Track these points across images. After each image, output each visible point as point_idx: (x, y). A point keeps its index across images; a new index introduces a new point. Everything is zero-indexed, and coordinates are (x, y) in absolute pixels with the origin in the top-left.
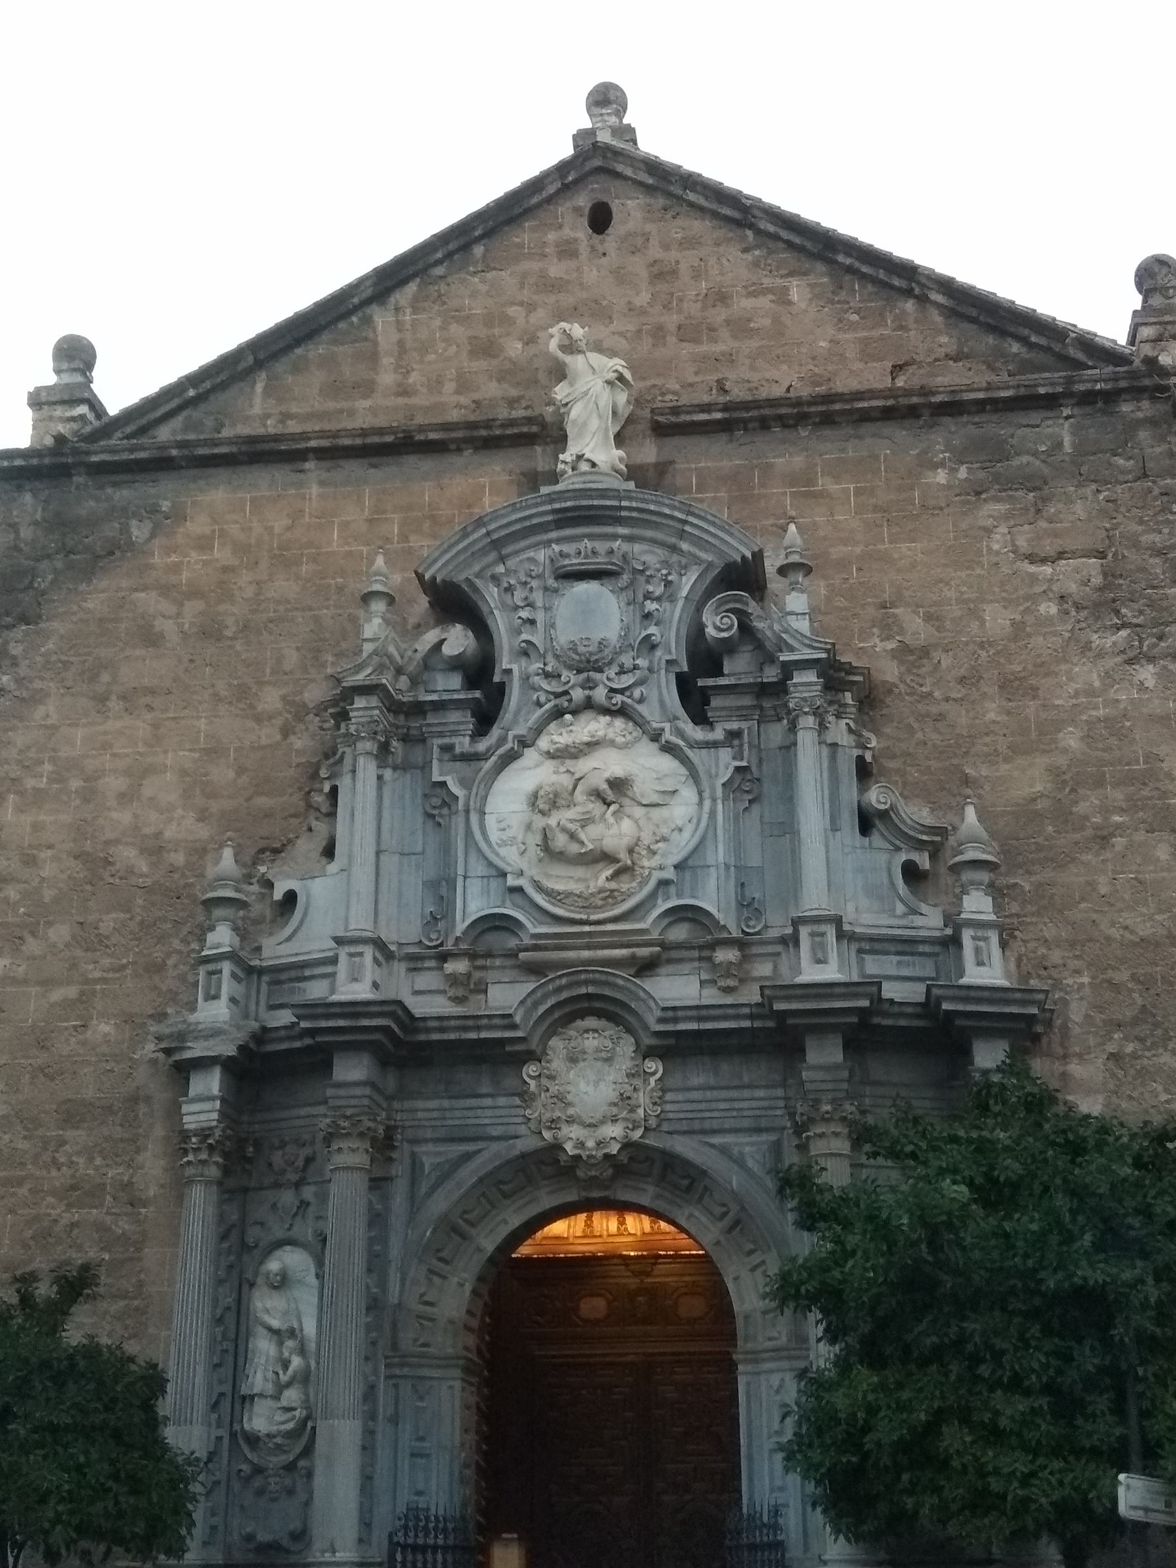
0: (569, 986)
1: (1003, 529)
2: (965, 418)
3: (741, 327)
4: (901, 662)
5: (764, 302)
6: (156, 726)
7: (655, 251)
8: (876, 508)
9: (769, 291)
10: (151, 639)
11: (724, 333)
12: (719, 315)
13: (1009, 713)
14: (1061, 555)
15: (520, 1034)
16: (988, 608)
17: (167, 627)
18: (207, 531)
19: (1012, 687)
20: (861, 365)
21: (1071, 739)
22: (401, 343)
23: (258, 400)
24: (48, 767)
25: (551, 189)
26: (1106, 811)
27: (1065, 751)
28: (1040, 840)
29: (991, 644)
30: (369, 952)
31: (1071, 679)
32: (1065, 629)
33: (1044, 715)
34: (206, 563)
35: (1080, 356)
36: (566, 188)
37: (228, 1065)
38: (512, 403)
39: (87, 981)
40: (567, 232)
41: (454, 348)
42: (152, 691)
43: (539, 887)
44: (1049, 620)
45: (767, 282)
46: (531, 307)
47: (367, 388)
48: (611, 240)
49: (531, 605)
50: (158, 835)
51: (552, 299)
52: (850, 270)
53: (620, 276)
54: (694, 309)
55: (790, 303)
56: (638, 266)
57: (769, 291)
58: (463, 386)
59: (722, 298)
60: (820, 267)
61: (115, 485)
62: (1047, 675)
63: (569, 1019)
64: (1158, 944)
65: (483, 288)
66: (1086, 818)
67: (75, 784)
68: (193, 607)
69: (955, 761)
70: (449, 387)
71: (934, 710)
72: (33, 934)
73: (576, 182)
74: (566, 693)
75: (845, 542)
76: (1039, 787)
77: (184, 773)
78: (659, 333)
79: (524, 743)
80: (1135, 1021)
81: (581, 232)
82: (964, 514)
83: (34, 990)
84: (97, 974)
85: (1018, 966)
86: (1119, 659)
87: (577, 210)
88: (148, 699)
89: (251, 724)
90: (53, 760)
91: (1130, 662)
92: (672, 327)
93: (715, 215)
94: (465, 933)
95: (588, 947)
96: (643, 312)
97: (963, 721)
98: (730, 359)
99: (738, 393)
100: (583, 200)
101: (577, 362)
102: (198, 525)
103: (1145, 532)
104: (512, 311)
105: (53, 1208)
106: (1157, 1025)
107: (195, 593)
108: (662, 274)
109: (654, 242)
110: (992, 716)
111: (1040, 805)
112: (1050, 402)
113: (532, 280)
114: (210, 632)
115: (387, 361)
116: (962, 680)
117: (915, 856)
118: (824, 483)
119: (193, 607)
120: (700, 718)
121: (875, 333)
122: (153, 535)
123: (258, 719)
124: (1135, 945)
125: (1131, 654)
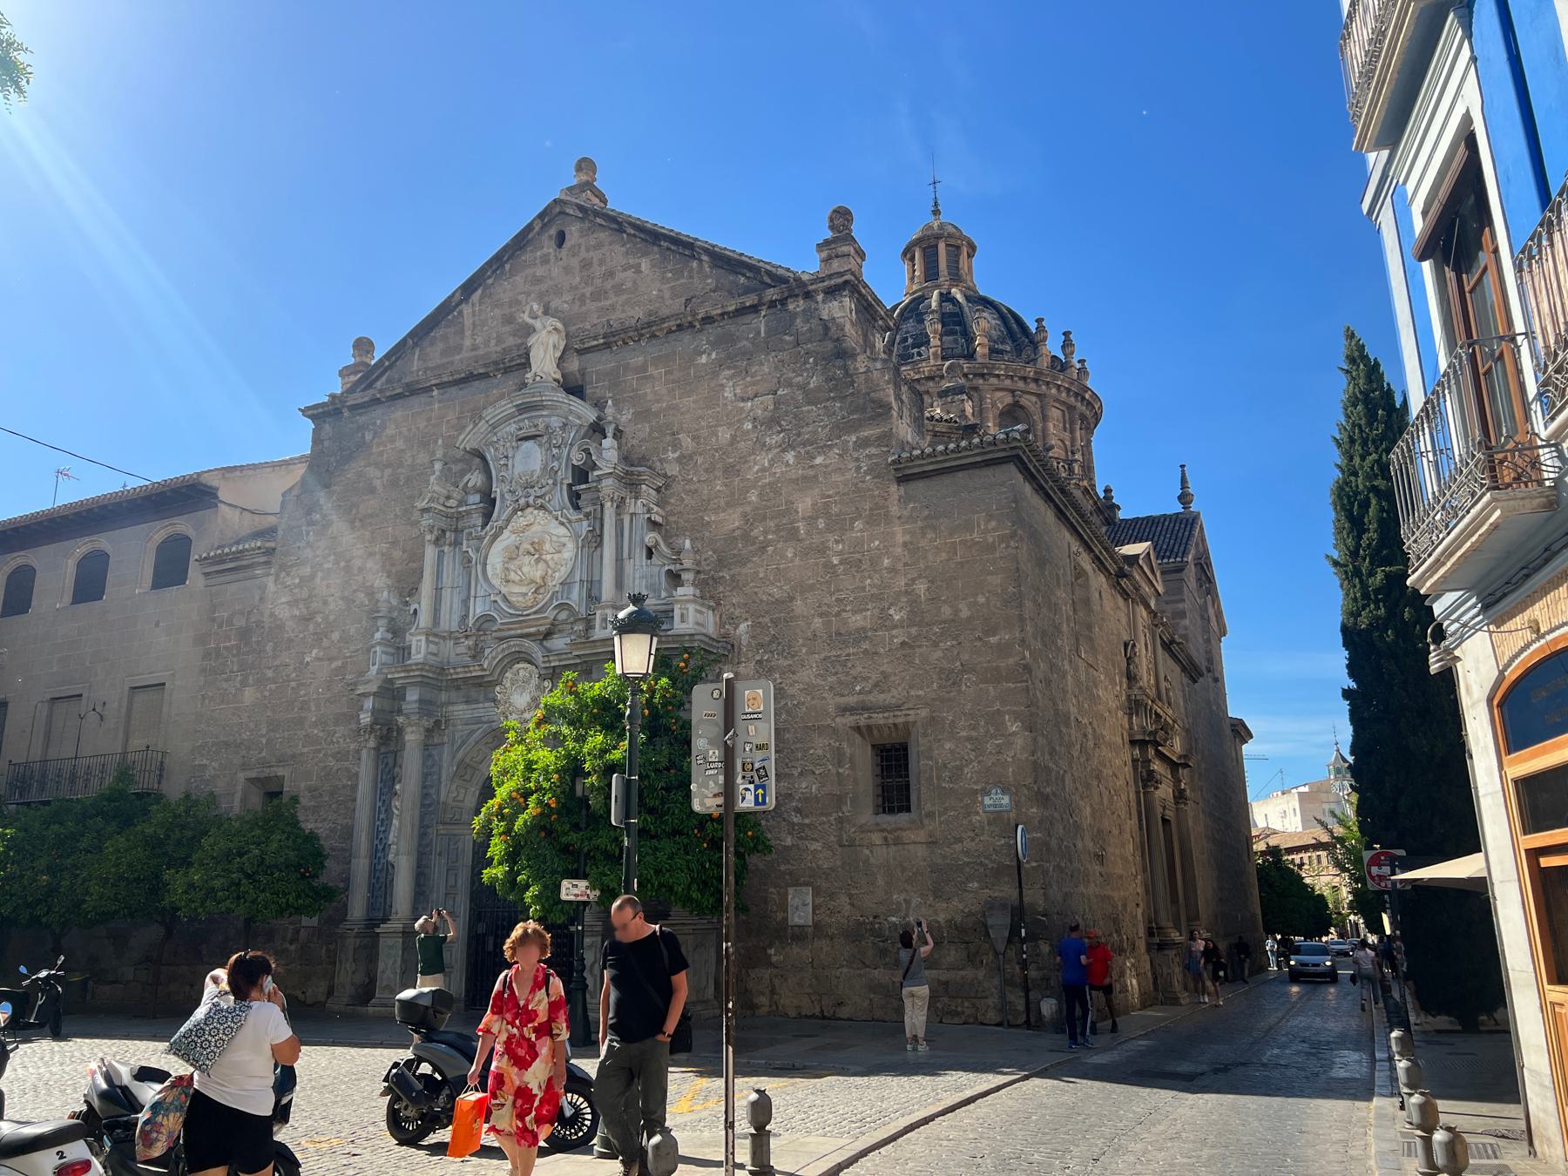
0: (508, 648)
1: (731, 384)
2: (716, 324)
3: (618, 289)
4: (681, 464)
5: (630, 273)
6: (373, 533)
7: (583, 254)
8: (673, 381)
9: (632, 267)
10: (372, 490)
11: (611, 294)
12: (609, 285)
13: (726, 486)
14: (756, 396)
15: (488, 673)
16: (720, 429)
17: (377, 483)
18: (394, 432)
19: (730, 471)
20: (671, 302)
21: (753, 497)
22: (474, 321)
23: (415, 363)
24: (332, 557)
25: (537, 229)
26: (765, 533)
27: (750, 503)
28: (735, 552)
29: (721, 449)
30: (423, 638)
31: (755, 464)
32: (753, 436)
33: (741, 485)
34: (392, 449)
35: (769, 281)
36: (545, 227)
37: (375, 694)
38: (518, 346)
39: (346, 658)
40: (545, 250)
41: (495, 322)
42: (371, 516)
43: (505, 599)
44: (748, 431)
45: (631, 261)
46: (528, 294)
47: (459, 349)
48: (564, 252)
49: (506, 457)
50: (372, 586)
51: (537, 288)
52: (669, 249)
53: (567, 270)
54: (598, 282)
55: (641, 272)
56: (575, 262)
57: (632, 267)
58: (499, 340)
59: (611, 274)
60: (656, 249)
61: (361, 414)
62: (744, 463)
63: (510, 665)
64: (783, 602)
65: (509, 287)
66: (757, 538)
67: (342, 564)
68: (388, 472)
69: (700, 514)
70: (493, 342)
71: (693, 487)
72: (326, 637)
73: (549, 221)
74: (517, 500)
75: (658, 401)
76: (737, 524)
77: (383, 555)
78: (582, 299)
79: (501, 529)
80: (771, 642)
81: (549, 247)
82: (712, 379)
83: (326, 663)
84: (348, 654)
85: (720, 618)
86: (778, 450)
87: (550, 237)
88: (368, 521)
89: (409, 527)
90: (334, 554)
91: (784, 451)
92: (588, 295)
93: (610, 229)
94: (474, 624)
95: (521, 628)
96: (576, 288)
97: (706, 492)
98: (613, 308)
99: (616, 325)
100: (553, 231)
101: (537, 324)
102: (391, 431)
103: (796, 376)
104: (520, 297)
105: (332, 763)
106: (779, 644)
107: (389, 465)
108: (586, 265)
109: (583, 248)
110: (718, 488)
111: (738, 533)
112: (754, 309)
113: (529, 279)
114: (394, 483)
115: (468, 333)
116: (706, 470)
117: (672, 567)
118: (651, 370)
119: (388, 472)
120: (577, 508)
121: (678, 283)
122: (374, 438)
123: (412, 526)
124: (773, 603)
125: (783, 446)
